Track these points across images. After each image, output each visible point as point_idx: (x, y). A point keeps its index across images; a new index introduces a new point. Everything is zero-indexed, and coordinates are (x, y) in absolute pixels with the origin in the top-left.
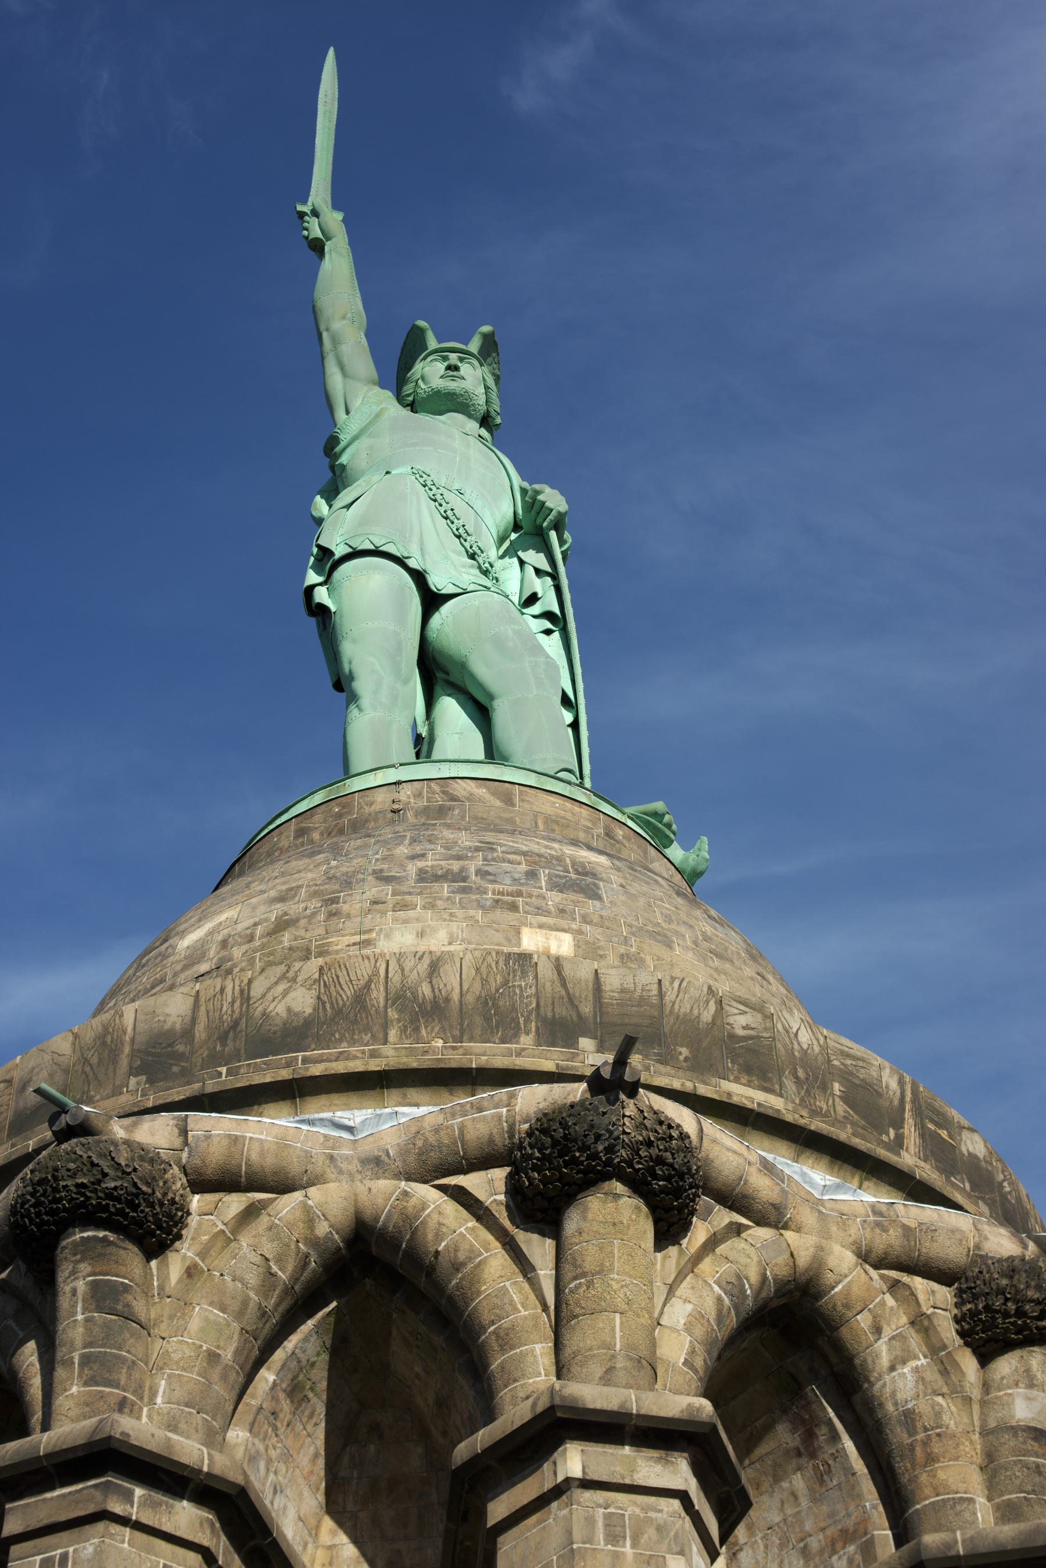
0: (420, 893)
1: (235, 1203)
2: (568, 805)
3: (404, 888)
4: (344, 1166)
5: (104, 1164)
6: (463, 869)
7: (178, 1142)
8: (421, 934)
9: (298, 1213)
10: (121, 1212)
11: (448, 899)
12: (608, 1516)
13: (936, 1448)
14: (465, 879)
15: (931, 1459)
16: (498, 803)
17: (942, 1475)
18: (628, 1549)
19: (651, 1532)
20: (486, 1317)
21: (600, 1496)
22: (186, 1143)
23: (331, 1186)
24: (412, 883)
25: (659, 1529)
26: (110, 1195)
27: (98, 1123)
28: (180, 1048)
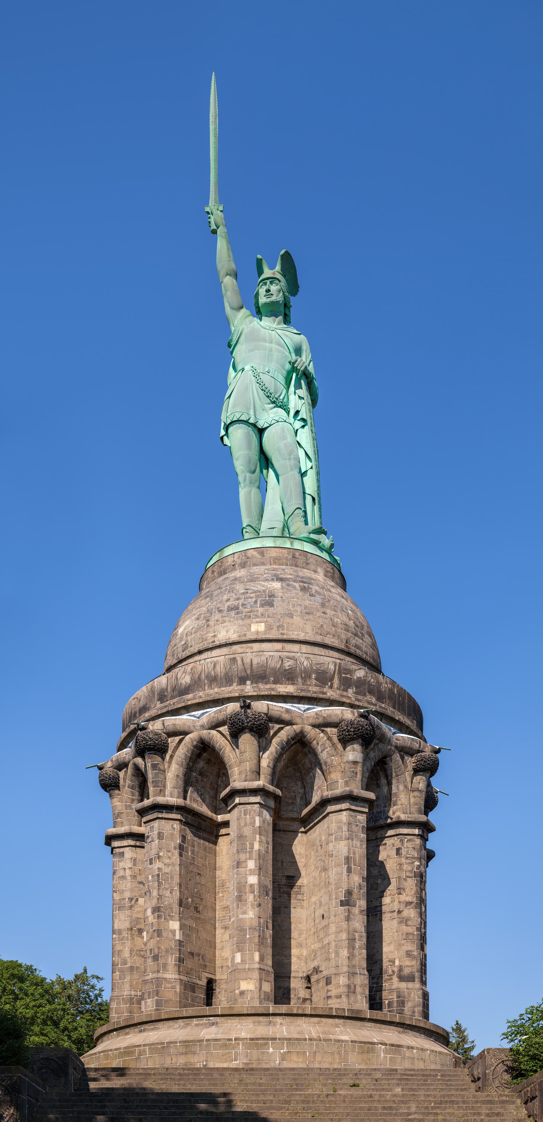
0: (227, 616)
1: (177, 739)
2: (281, 550)
3: (224, 615)
4: (197, 728)
5: (147, 738)
6: (238, 604)
7: (163, 728)
8: (227, 631)
9: (190, 740)
10: (153, 748)
11: (234, 617)
12: (244, 810)
13: (331, 770)
14: (238, 609)
15: (330, 772)
16: (260, 557)
17: (332, 776)
18: (248, 816)
19: (253, 812)
20: (227, 762)
21: (243, 806)
22: (164, 727)
23: (195, 733)
24: (225, 612)
25: (255, 811)
26: (150, 745)
27: (145, 726)
28: (166, 693)
